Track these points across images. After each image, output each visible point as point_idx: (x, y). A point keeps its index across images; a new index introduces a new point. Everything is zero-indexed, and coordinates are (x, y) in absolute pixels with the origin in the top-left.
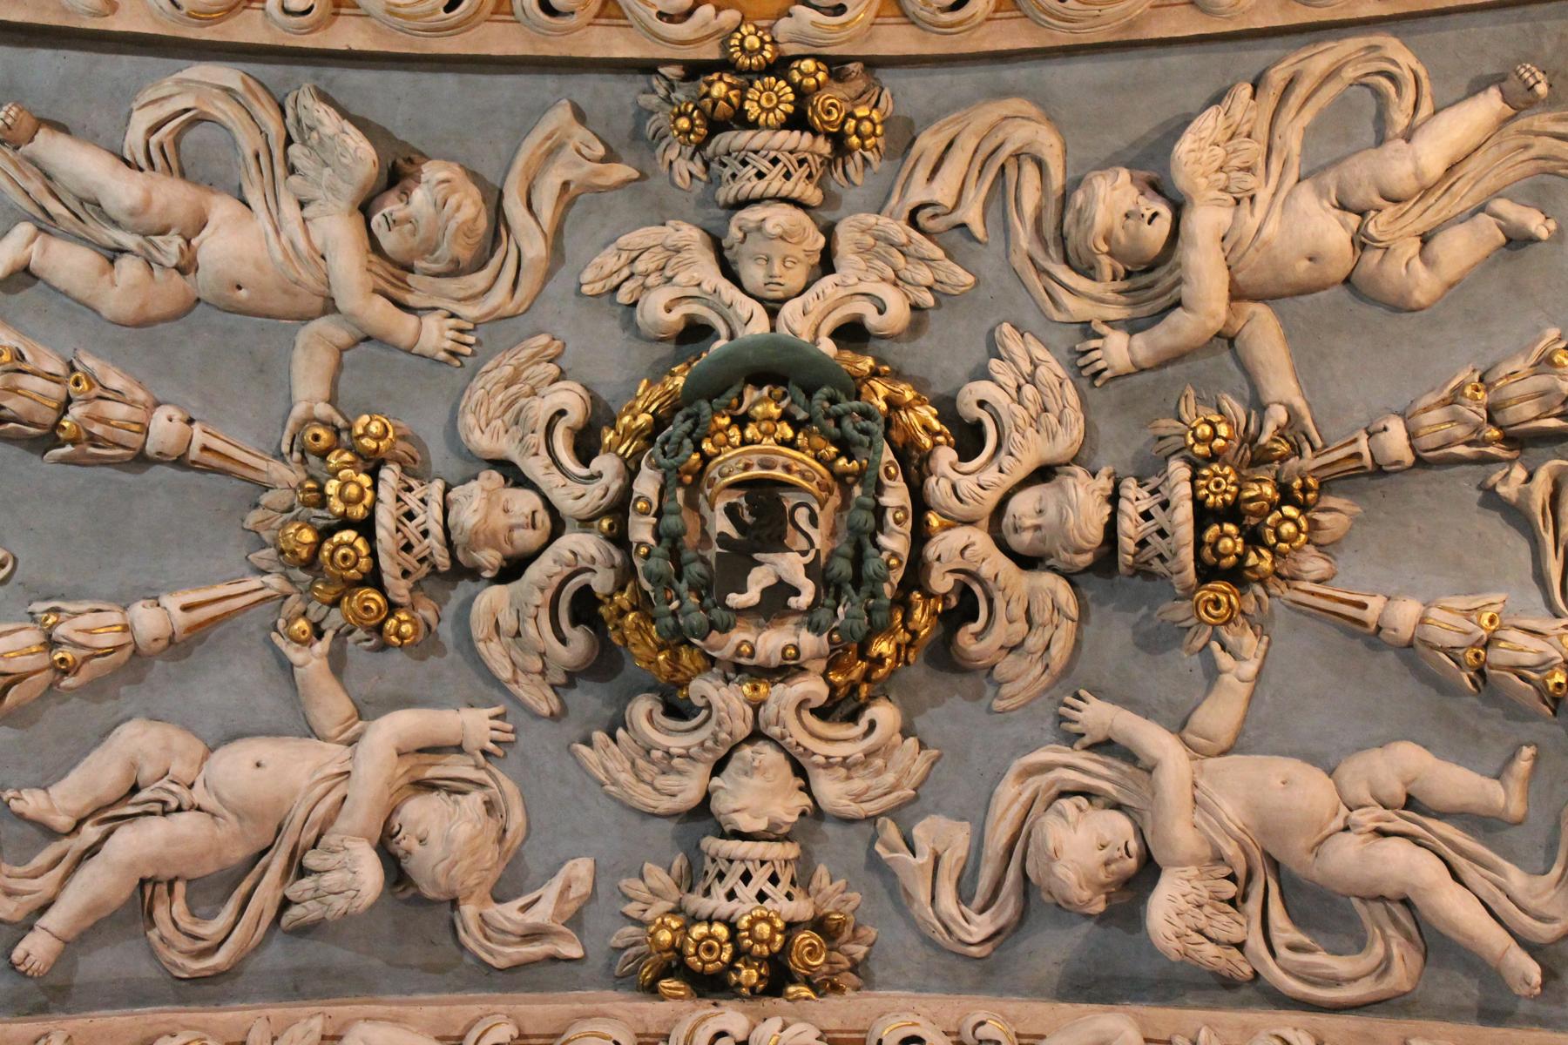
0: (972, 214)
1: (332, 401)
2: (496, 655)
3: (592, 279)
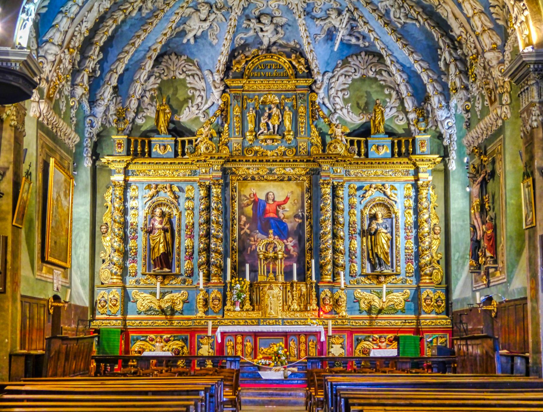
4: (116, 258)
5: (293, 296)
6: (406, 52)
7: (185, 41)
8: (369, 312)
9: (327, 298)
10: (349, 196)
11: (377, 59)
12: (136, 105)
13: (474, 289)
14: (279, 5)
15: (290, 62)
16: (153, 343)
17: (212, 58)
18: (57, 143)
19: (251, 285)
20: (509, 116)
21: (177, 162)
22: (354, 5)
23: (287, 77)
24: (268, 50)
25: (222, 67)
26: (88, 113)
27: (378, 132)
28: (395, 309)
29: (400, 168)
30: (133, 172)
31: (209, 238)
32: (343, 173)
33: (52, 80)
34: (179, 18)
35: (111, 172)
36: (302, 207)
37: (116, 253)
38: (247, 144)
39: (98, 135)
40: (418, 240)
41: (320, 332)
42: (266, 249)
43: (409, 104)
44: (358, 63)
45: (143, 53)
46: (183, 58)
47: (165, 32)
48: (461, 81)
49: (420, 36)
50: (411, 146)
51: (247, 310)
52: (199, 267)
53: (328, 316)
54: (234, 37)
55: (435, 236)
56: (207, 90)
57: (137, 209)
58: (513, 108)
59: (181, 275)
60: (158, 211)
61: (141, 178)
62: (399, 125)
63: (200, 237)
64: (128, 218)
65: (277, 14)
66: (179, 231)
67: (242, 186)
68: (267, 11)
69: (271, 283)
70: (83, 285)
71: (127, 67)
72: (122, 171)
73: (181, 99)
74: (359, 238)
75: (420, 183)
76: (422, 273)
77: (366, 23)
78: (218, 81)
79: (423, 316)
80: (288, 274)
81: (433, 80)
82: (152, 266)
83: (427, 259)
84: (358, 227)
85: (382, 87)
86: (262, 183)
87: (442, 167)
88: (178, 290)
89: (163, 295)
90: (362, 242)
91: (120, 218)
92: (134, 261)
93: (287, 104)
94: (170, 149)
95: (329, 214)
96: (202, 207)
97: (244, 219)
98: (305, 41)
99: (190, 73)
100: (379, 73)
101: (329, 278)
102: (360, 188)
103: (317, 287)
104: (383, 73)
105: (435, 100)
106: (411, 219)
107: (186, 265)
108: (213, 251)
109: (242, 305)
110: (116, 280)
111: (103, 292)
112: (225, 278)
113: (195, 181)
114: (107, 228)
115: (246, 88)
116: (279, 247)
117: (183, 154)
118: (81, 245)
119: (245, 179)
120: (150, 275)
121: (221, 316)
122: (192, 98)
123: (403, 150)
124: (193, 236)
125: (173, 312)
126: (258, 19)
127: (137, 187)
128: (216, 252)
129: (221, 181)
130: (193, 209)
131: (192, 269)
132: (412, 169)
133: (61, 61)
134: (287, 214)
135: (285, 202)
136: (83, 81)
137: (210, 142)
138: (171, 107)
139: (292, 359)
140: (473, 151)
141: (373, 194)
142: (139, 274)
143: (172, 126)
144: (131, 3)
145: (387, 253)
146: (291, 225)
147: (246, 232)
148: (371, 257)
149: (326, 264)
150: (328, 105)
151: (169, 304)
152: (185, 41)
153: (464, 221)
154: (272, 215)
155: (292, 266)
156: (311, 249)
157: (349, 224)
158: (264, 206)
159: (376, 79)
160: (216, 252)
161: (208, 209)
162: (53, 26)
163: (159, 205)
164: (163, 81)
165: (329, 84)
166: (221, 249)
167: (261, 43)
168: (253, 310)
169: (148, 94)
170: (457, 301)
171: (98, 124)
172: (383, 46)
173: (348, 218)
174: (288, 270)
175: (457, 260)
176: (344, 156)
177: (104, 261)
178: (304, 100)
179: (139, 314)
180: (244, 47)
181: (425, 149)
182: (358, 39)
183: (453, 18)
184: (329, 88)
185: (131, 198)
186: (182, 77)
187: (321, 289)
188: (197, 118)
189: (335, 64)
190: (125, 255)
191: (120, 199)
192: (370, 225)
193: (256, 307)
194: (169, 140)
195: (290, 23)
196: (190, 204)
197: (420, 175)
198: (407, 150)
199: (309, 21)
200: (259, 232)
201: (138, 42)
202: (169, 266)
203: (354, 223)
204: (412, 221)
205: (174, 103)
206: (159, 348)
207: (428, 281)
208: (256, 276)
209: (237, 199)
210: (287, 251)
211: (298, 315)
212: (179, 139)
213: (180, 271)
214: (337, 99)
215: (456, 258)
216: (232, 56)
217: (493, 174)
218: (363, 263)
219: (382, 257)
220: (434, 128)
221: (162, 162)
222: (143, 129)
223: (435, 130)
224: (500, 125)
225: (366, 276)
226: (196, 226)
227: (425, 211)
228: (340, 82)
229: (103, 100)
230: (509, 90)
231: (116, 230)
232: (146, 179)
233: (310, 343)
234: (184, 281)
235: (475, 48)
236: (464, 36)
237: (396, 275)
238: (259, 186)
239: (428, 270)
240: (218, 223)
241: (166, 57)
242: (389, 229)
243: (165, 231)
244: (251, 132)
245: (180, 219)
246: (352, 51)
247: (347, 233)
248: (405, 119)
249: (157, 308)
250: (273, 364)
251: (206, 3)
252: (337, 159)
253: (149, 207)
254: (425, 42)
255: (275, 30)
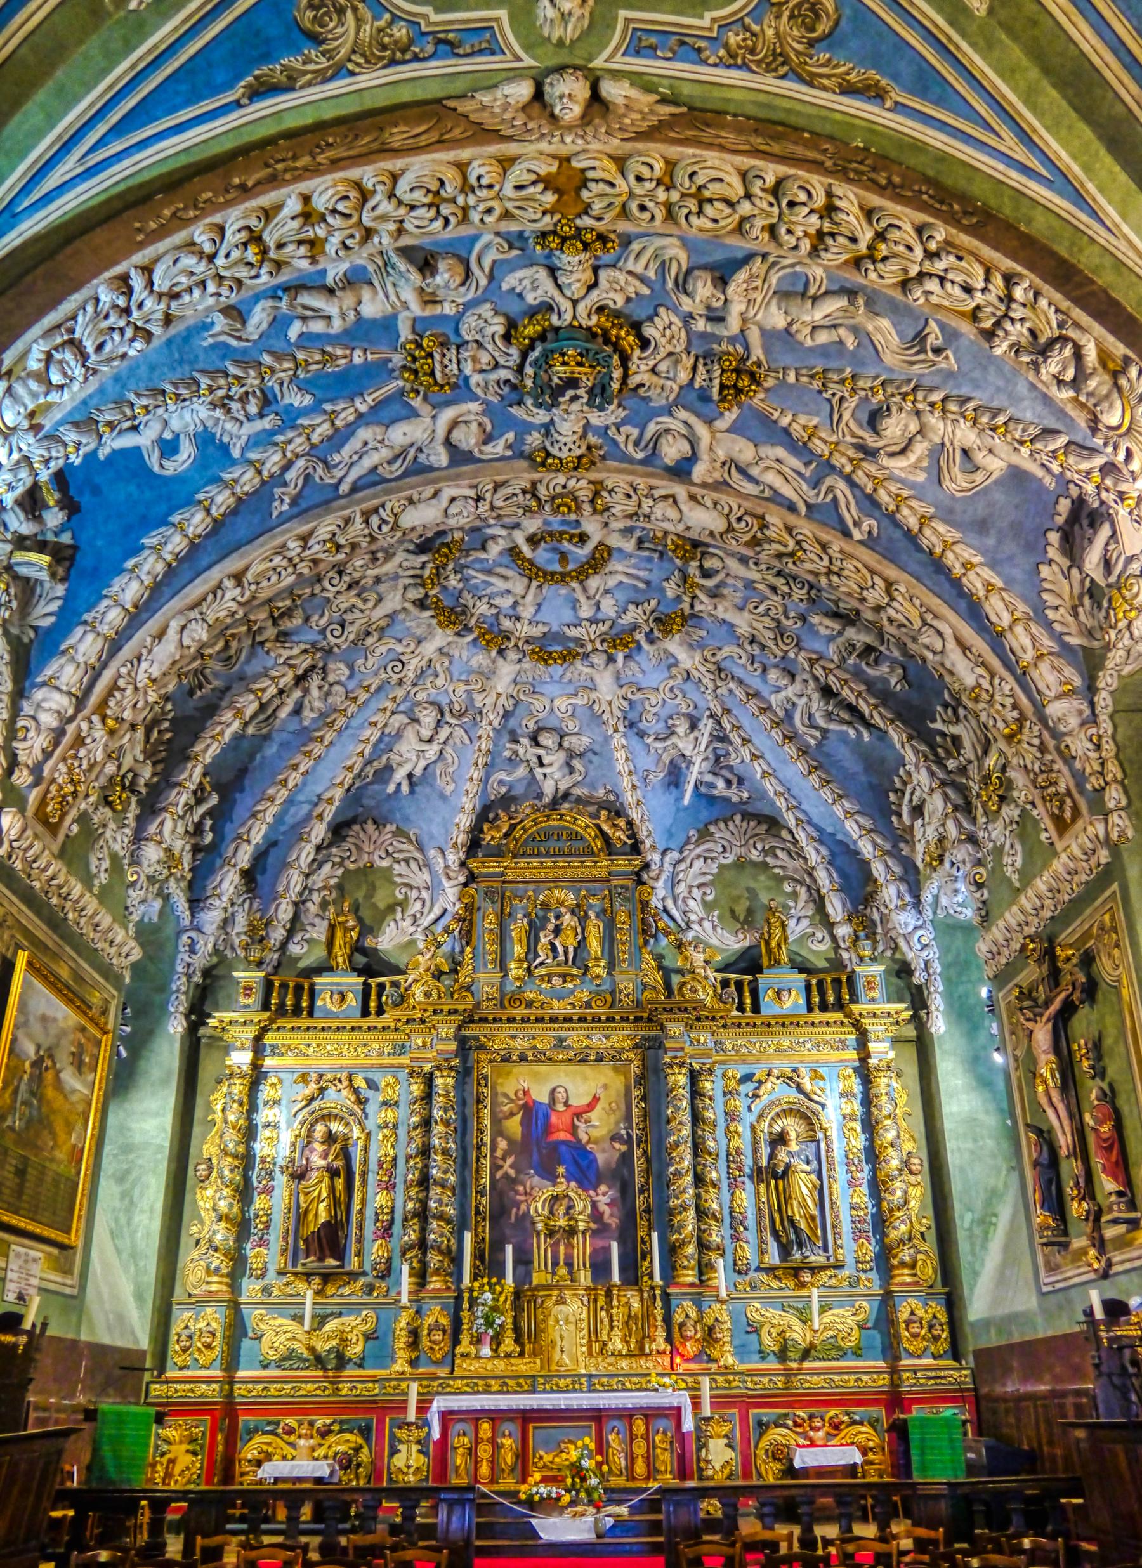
0: (651, 274)
1: (414, 332)
2: (479, 391)
3: (505, 287)
4: (222, 1234)
5: (611, 1320)
6: (827, 794)
7: (391, 788)
8: (782, 1355)
9: (690, 1323)
10: (725, 1094)
11: (764, 827)
12: (290, 915)
13: (1045, 1289)
14: (574, 706)
15: (598, 827)
16: (292, 1438)
17: (446, 824)
18: (62, 937)
19: (517, 1294)
20: (1130, 833)
21: (365, 1026)
22: (722, 703)
23: (592, 854)
24: (555, 803)
25: (462, 838)
26: (187, 922)
27: (778, 963)
28: (840, 1348)
29: (828, 1034)
30: (273, 1047)
31: (427, 1189)
32: (711, 1045)
33: (53, 781)
34: (377, 734)
35: (227, 1050)
36: (628, 1117)
37: (223, 1224)
38: (510, 987)
39: (207, 973)
40: (877, 1188)
41: (679, 1409)
42: (551, 1212)
43: (836, 908)
44: (728, 835)
45: (306, 808)
46: (389, 828)
47: (349, 763)
48: (960, 826)
49: (852, 764)
50: (845, 990)
51: (508, 1356)
52: (404, 1254)
53: (693, 1366)
54: (488, 777)
55: (912, 1179)
56: (434, 888)
57: (276, 1126)
58: (1137, 814)
59: (364, 1274)
60: (320, 1128)
61: (288, 1061)
62: (819, 949)
63: (408, 1186)
64: (257, 1146)
65: (571, 726)
66: (364, 1174)
67: (499, 1075)
68: (553, 722)
69: (561, 1288)
70: (139, 1297)
71: (273, 838)
72: (248, 1044)
73: (382, 905)
74: (749, 1185)
75: (873, 1062)
76: (895, 1262)
77: (746, 741)
78: (455, 867)
79: (906, 1362)
80: (600, 1268)
81: (887, 853)
82: (301, 1254)
83: (903, 1228)
84: (748, 1161)
85: (779, 880)
86: (542, 1069)
87: (910, 1032)
88: (354, 1308)
89: (321, 1320)
90: (758, 1194)
91: (238, 1144)
92: (263, 1243)
93: (591, 906)
94: (352, 1000)
95: (686, 1131)
96: (415, 1119)
97: (503, 1144)
98: (626, 782)
99: (400, 856)
100: (771, 852)
101: (690, 1276)
102: (747, 1078)
103: (666, 1297)
104: (779, 852)
105: (890, 893)
106: (859, 1142)
107: (375, 1250)
108: (434, 1217)
109: (497, 1340)
110: (217, 1286)
111: (187, 1314)
112: (459, 1279)
113: (400, 1066)
114: (210, 1169)
115: (511, 877)
116: (579, 1206)
117: (380, 1011)
118: (144, 1204)
119: (505, 1059)
120: (295, 1274)
121: (447, 1370)
122: (403, 904)
123: (831, 999)
124: (394, 1186)
125: (342, 1362)
126: (535, 740)
127: (280, 1081)
128: (441, 1217)
129: (456, 1062)
130: (395, 1126)
131: (389, 1260)
132: (851, 1037)
133: (79, 741)
134: (595, 1133)
135: (591, 1107)
136: (161, 833)
137: (435, 982)
138: (360, 920)
139: (616, 1482)
140: (1024, 947)
141: (775, 1091)
142: (271, 1273)
143: (360, 960)
144: (272, 679)
145: (813, 1218)
146: (605, 1156)
147: (506, 1175)
148: (778, 1227)
149: (683, 1244)
150: (674, 912)
151: (334, 1343)
152: (391, 788)
153: (975, 1141)
154: (563, 1136)
155: (608, 1249)
156: (648, 1210)
157: (728, 1154)
158: (547, 1117)
159: (765, 866)
160: (441, 1217)
161: (427, 1123)
162: (63, 652)
163: (323, 1118)
164: (347, 871)
165: (674, 874)
166: (451, 1211)
167: (540, 796)
168: (521, 1354)
169: (316, 897)
170: (986, 1323)
171: (205, 946)
172: (780, 789)
173: (723, 1142)
174: (600, 1259)
175: (970, 1229)
176: (711, 1009)
177: (198, 1242)
178: (627, 899)
179: (265, 1367)
180: (507, 801)
181: (876, 994)
182: (729, 783)
183: (958, 651)
184: (674, 882)
185: (266, 1103)
186: (385, 864)
187: (674, 1303)
188: (412, 943)
189: (683, 839)
190: (242, 1228)
191: (241, 1104)
192: (772, 1156)
193: (528, 1347)
194: (355, 982)
195: (597, 748)
196: (390, 1115)
197: (872, 1047)
198: (839, 999)
199: (635, 741)
200: (537, 1173)
201: (294, 778)
202: (339, 1253)
203: (739, 1152)
204: (861, 1146)
205: (365, 913)
206: (305, 1452)
207: (908, 1279)
208: (528, 1275)
209: (488, 1101)
210: (596, 1215)
211: (624, 1364)
212: (373, 981)
213: (361, 1264)
214: (691, 903)
215: (967, 1225)
216: (485, 815)
217: (1091, 990)
218: (762, 1241)
219: (803, 1225)
220: (889, 953)
221: (334, 1025)
222: (302, 964)
223: (892, 959)
224: (1103, 861)
225: (770, 1270)
226: (401, 1162)
227: (888, 1122)
228: (696, 871)
229: (219, 896)
230: (1119, 776)
231: (227, 1172)
232: (301, 1061)
233: (658, 1438)
234: (370, 1289)
235: (1015, 707)
236: (985, 684)
237: (836, 1267)
238: (536, 1075)
239: (905, 1254)
240: (445, 1152)
241: (357, 827)
242: (815, 1165)
243: (333, 1173)
244: (520, 960)
245: (366, 1149)
246: (716, 812)
247: (724, 1175)
248: (828, 939)
249: (306, 1354)
250: (567, 1498)
251: (432, 703)
252: (697, 1016)
253: (302, 1123)
254: (863, 778)
255: (568, 764)
